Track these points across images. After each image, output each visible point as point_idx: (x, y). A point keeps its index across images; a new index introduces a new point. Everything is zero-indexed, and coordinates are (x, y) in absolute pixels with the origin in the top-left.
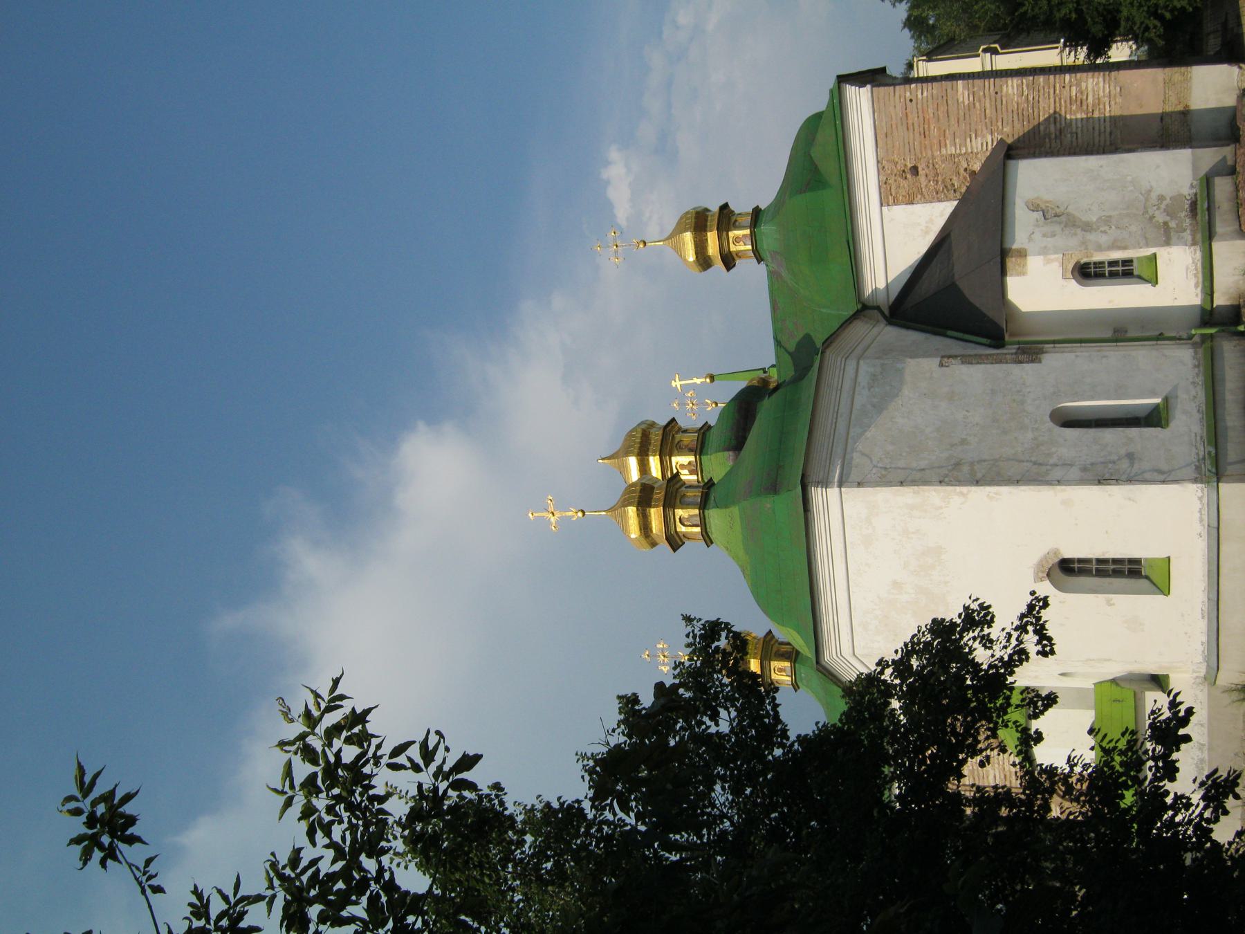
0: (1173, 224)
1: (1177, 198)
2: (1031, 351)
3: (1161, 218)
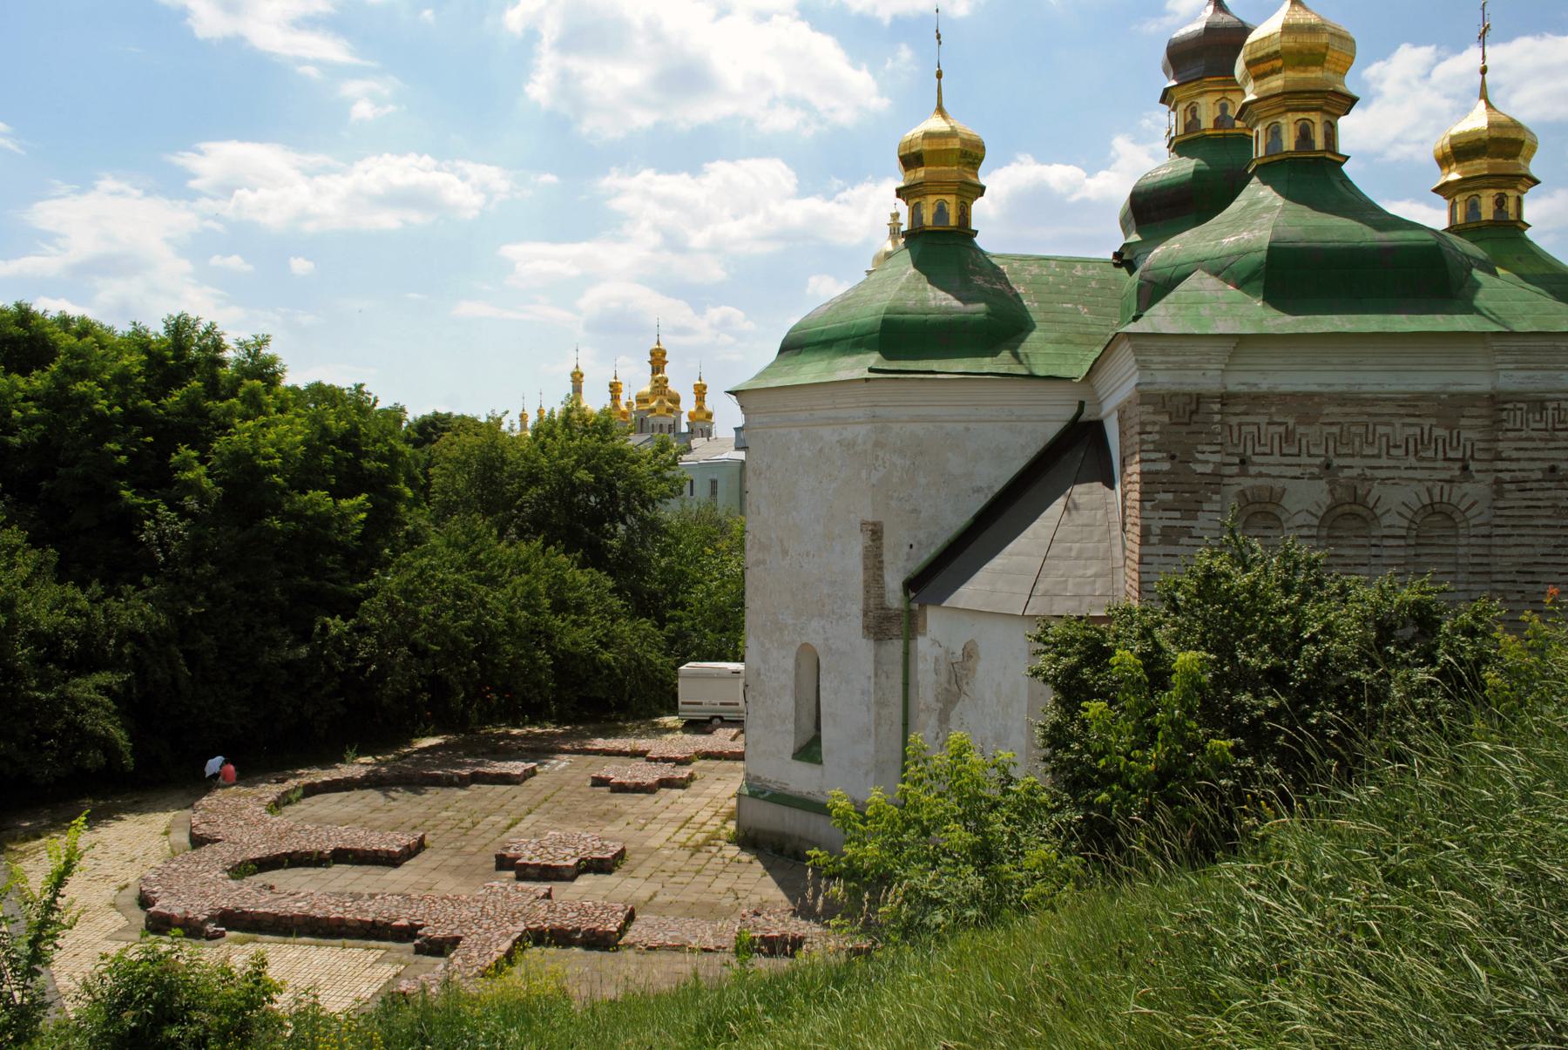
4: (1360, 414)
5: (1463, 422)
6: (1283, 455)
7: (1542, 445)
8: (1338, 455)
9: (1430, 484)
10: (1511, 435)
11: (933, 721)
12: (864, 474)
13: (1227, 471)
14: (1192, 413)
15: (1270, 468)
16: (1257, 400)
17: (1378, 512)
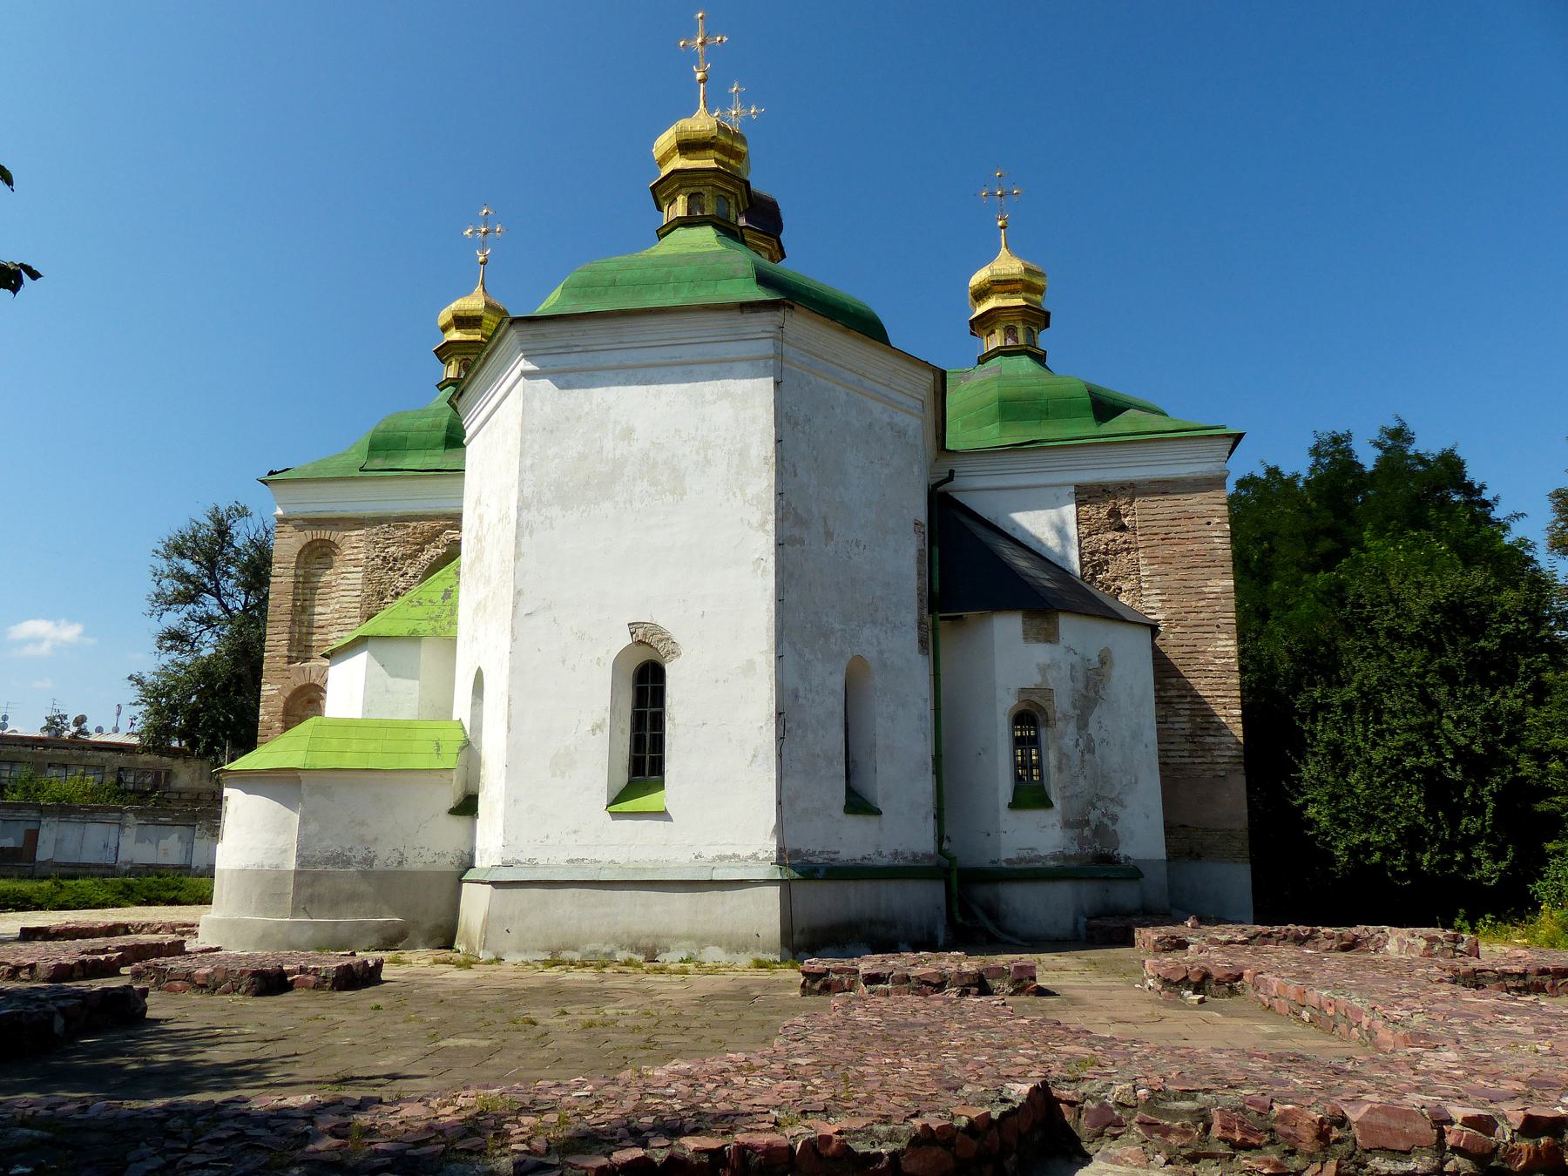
0: (1087, 832)
1: (1114, 840)
2: (930, 643)
3: (1094, 816)
11: (1072, 728)
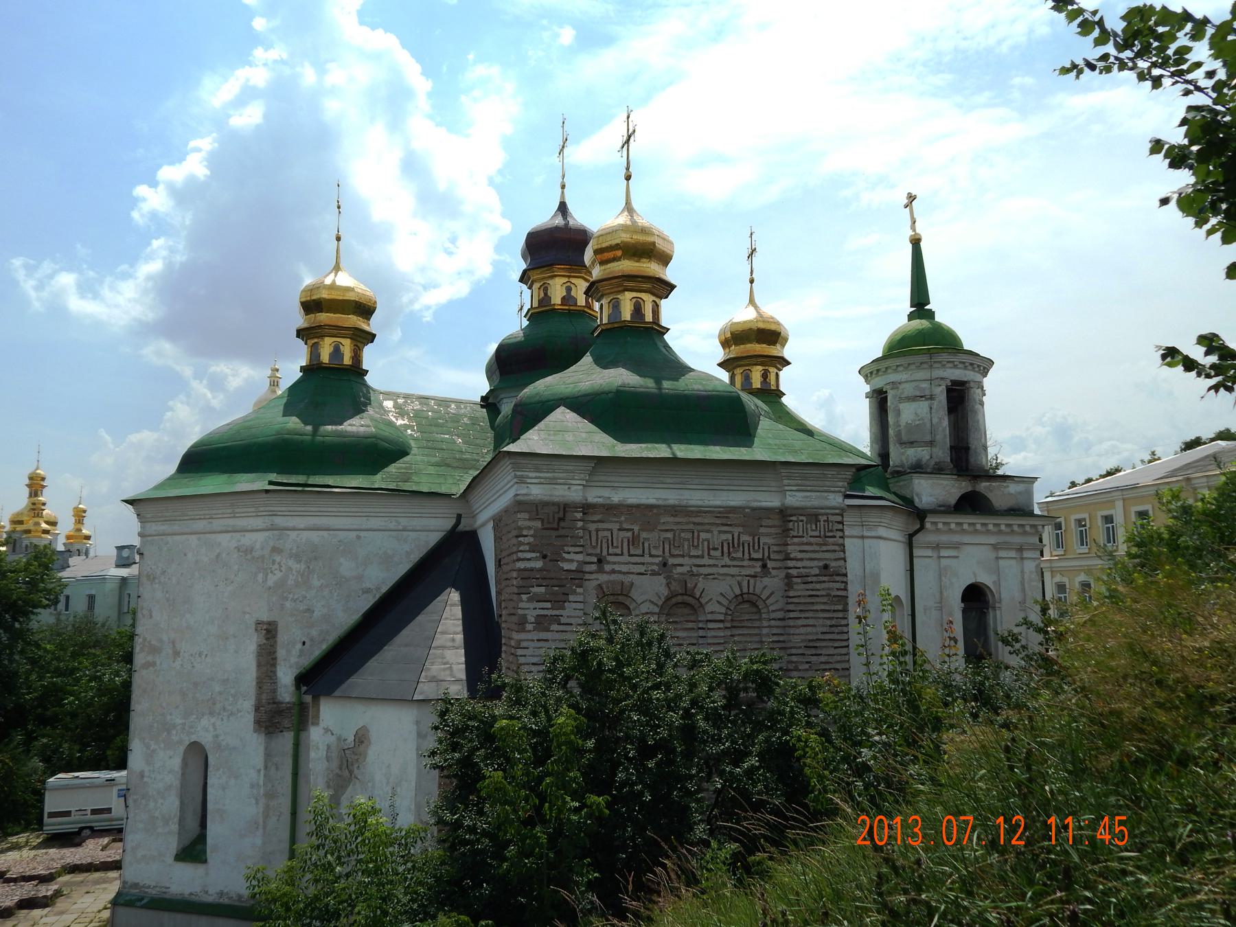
4: (687, 523)
5: (762, 530)
6: (630, 555)
7: (817, 548)
8: (673, 556)
9: (739, 578)
10: (796, 540)
12: (260, 576)
13: (588, 568)
14: (561, 519)
15: (622, 565)
16: (610, 509)
17: (703, 601)
